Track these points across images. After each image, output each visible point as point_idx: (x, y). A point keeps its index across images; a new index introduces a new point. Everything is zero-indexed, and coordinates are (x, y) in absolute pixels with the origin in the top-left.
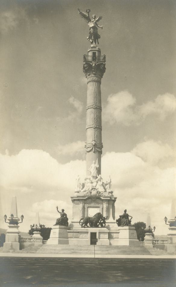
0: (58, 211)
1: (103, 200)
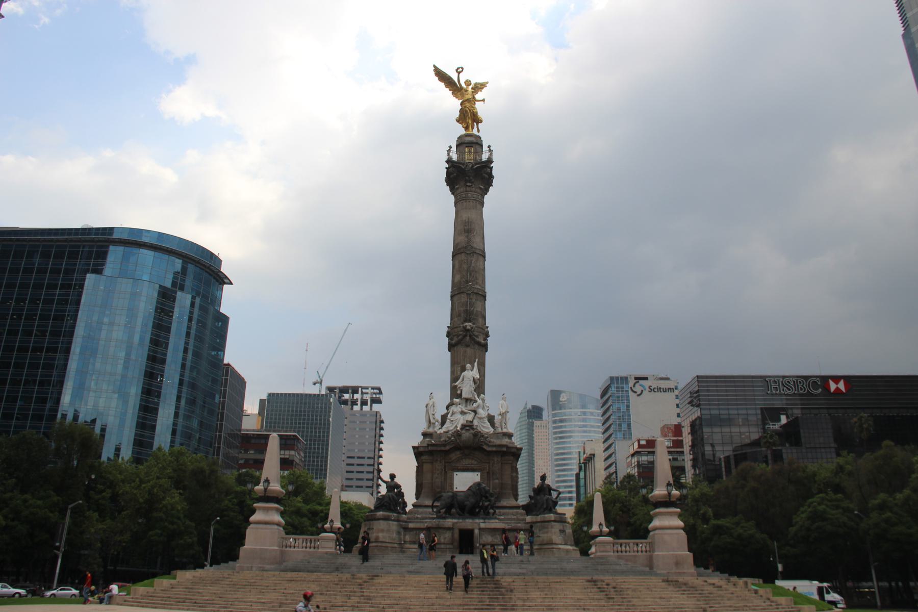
1: (489, 453)
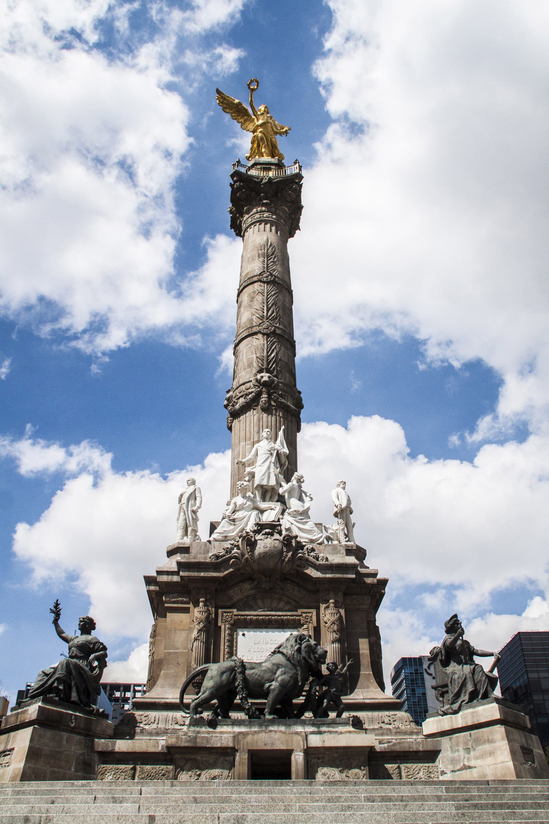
0: (60, 633)
